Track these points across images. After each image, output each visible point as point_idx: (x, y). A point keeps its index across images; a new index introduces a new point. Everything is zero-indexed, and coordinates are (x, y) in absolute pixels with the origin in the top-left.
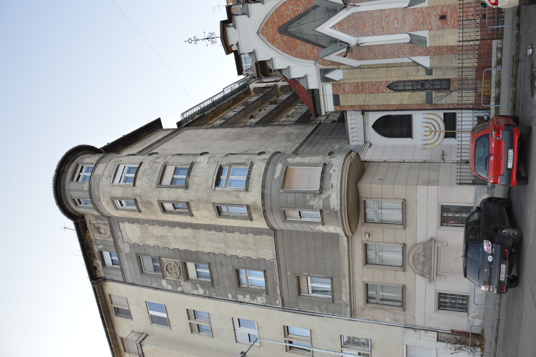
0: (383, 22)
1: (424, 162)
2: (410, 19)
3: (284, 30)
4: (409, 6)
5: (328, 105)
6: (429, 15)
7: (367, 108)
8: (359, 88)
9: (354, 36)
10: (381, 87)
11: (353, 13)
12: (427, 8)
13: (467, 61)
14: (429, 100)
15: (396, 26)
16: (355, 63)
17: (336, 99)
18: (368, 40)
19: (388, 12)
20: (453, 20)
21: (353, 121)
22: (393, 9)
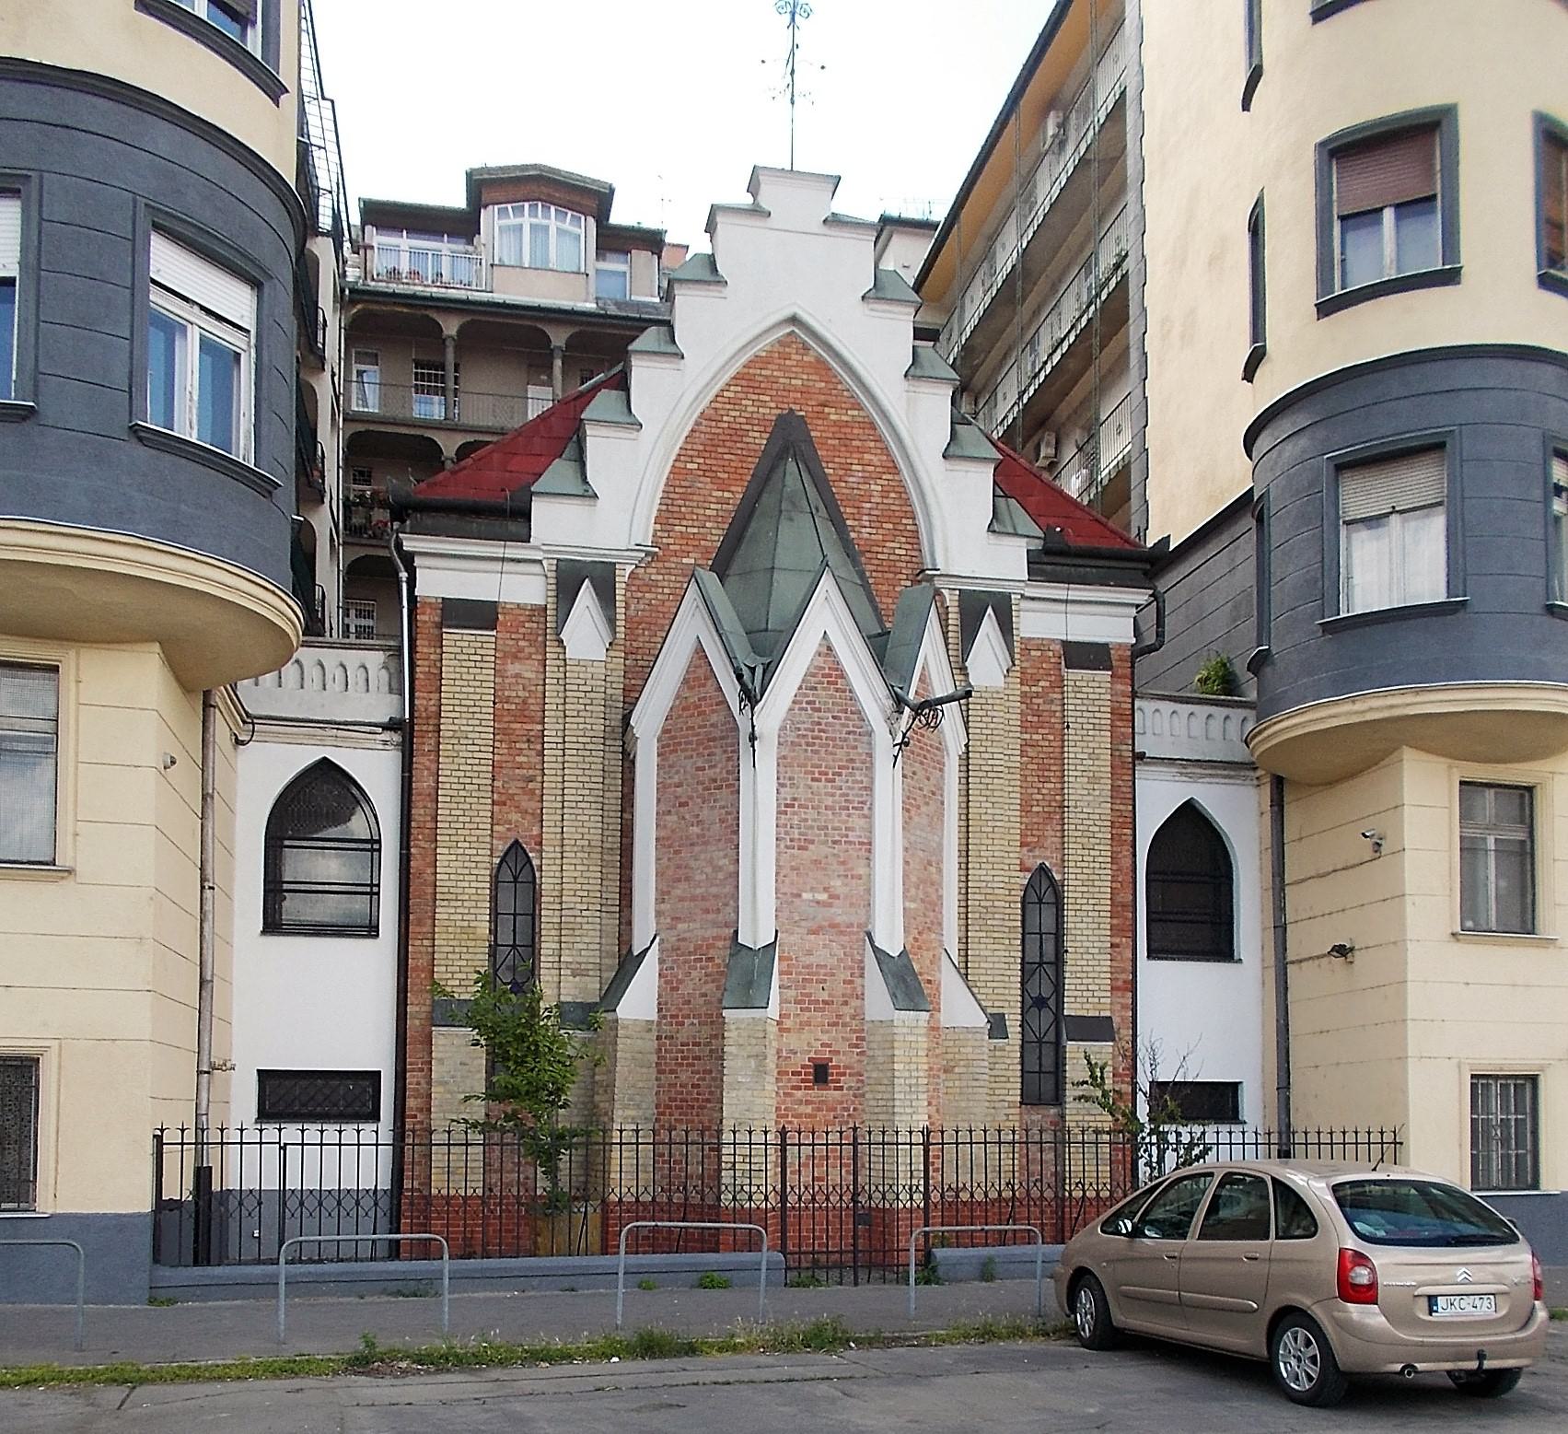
0: (825, 850)
1: (202, 982)
2: (825, 952)
4: (876, 950)
5: (445, 571)
6: (836, 1024)
7: (423, 745)
8: (518, 722)
9: (783, 728)
10: (515, 817)
11: (870, 734)
12: (858, 1015)
13: (629, 1163)
14: (447, 1012)
15: (805, 896)
16: (649, 719)
18: (761, 785)
19: (862, 871)
20: (809, 1110)
21: (355, 676)
22: (869, 891)
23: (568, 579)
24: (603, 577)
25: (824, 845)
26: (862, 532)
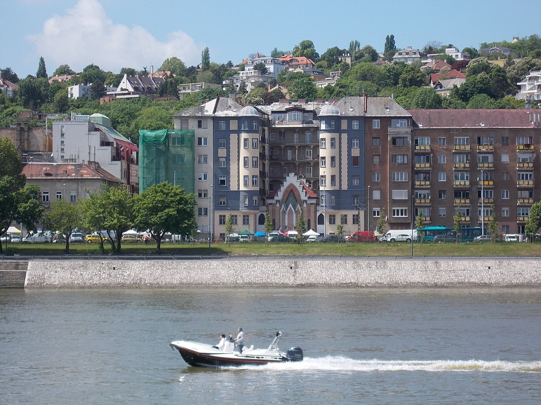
3: (292, 191)
5: (269, 201)
8: (274, 211)
16: (281, 211)
17: (271, 204)
18: (287, 216)
23: (277, 201)
24: (279, 201)
25: (290, 219)
26: (296, 196)
